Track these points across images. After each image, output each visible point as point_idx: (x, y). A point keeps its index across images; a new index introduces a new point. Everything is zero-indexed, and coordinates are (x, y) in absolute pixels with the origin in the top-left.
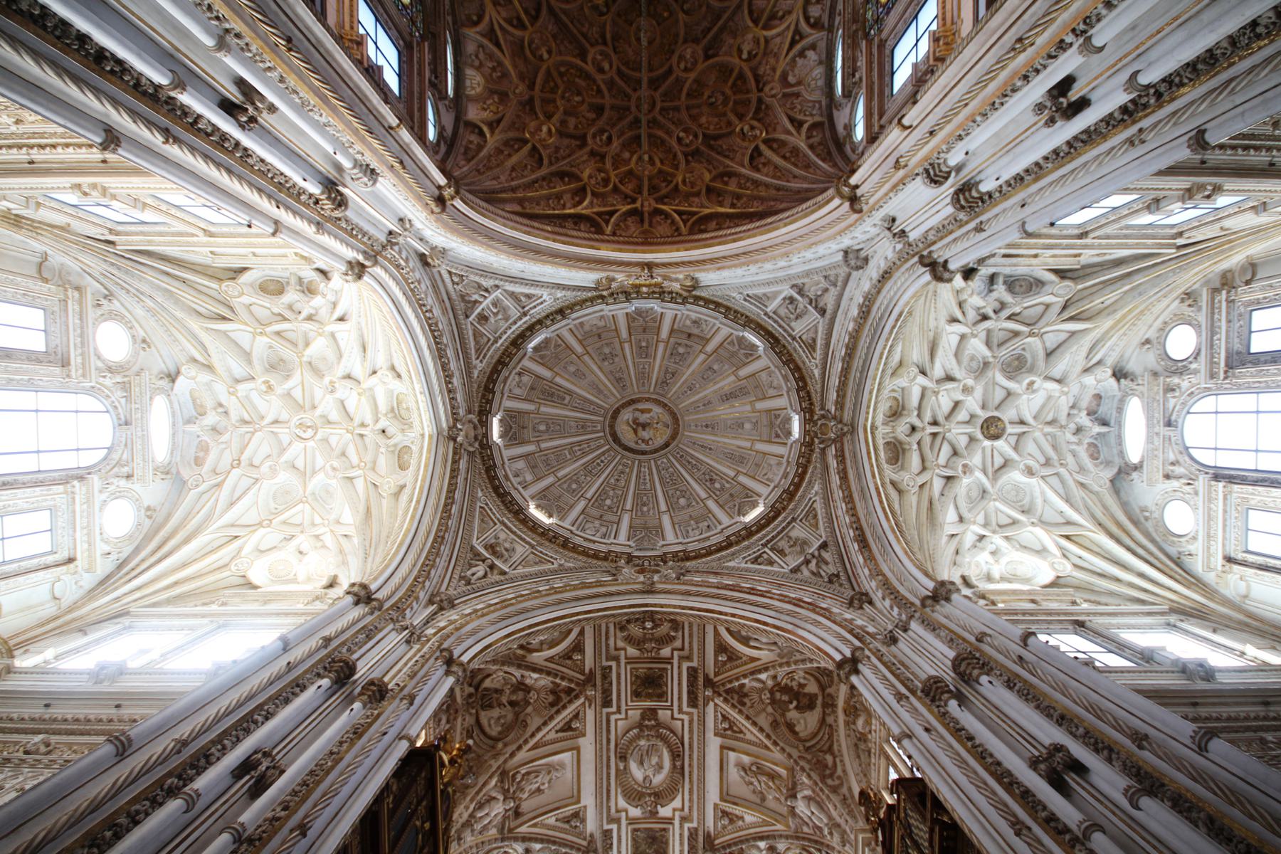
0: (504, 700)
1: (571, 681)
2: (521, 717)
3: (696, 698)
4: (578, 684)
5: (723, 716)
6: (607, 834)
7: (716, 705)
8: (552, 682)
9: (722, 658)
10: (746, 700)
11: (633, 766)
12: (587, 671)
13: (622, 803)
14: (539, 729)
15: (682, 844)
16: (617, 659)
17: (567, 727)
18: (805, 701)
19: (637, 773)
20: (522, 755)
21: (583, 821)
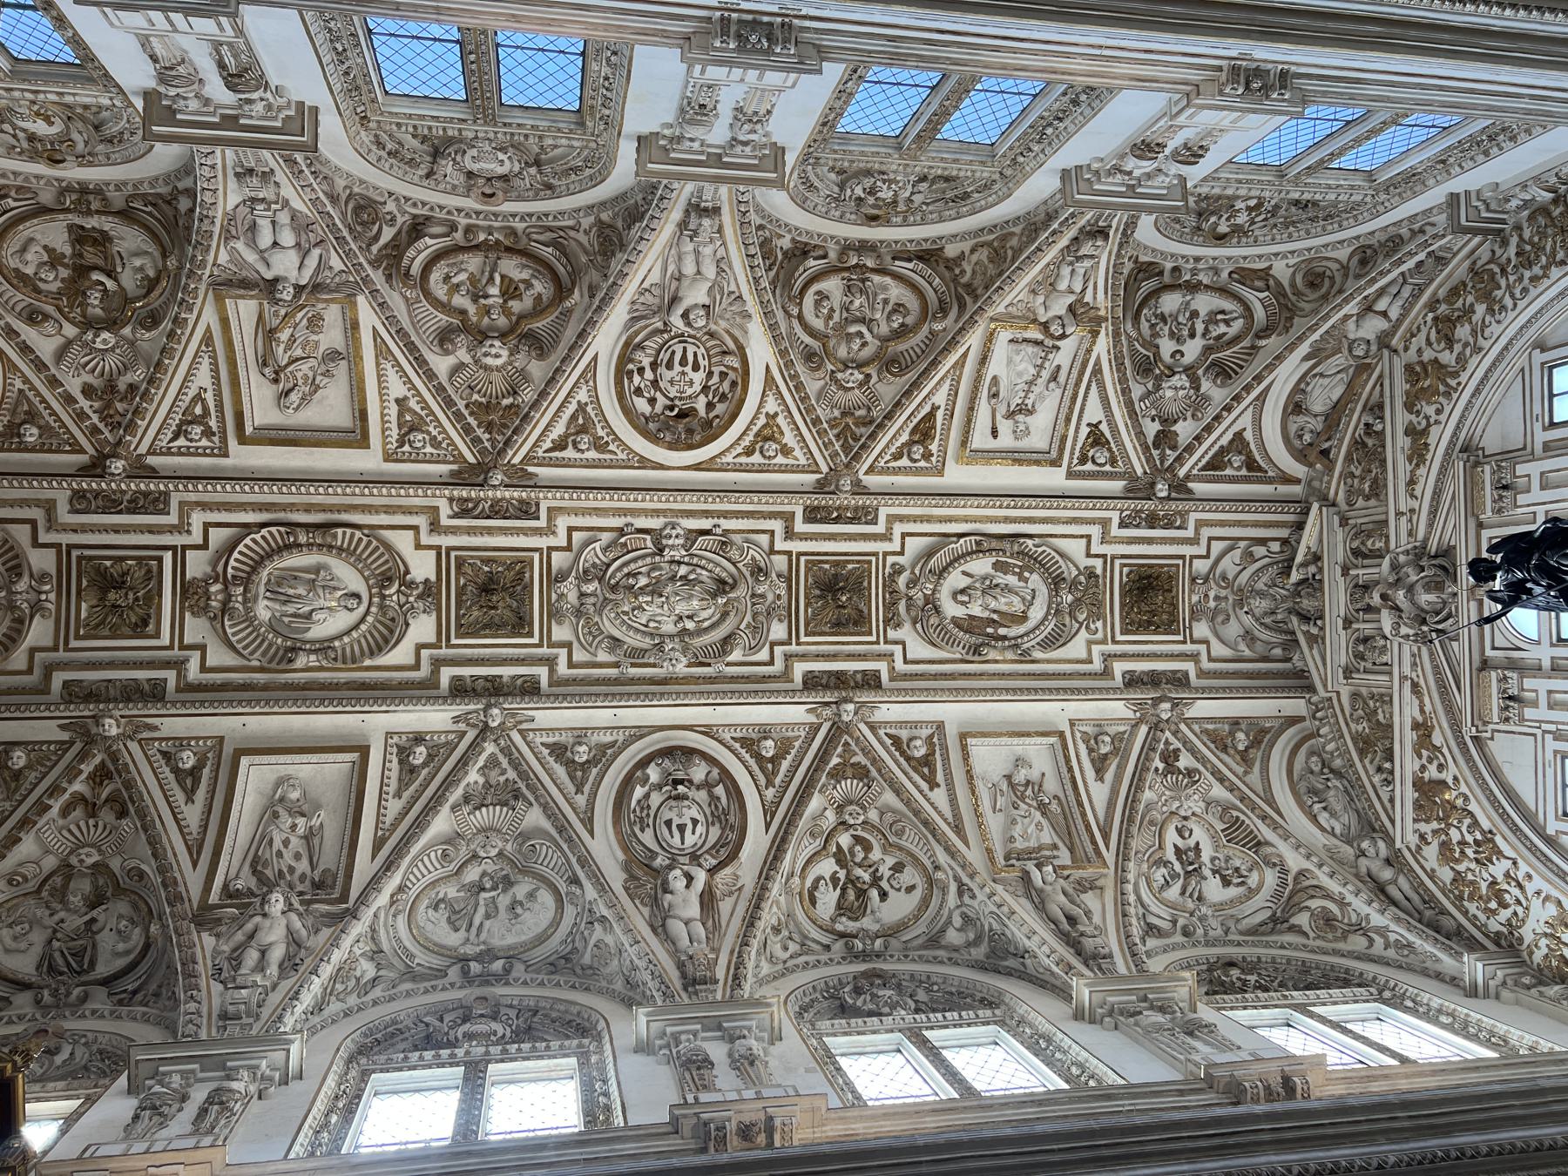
0: (75, 922)
1: (72, 773)
2: (125, 882)
3: (146, 494)
4: (83, 756)
5: (176, 437)
6: (460, 690)
7: (152, 451)
8: (65, 812)
9: (31, 434)
10: (122, 384)
11: (317, 632)
12: (65, 736)
13: (400, 654)
14: (153, 842)
15: (490, 531)
16: (49, 670)
17: (189, 779)
18: (91, 256)
19: (331, 623)
20: (193, 880)
21: (418, 738)
